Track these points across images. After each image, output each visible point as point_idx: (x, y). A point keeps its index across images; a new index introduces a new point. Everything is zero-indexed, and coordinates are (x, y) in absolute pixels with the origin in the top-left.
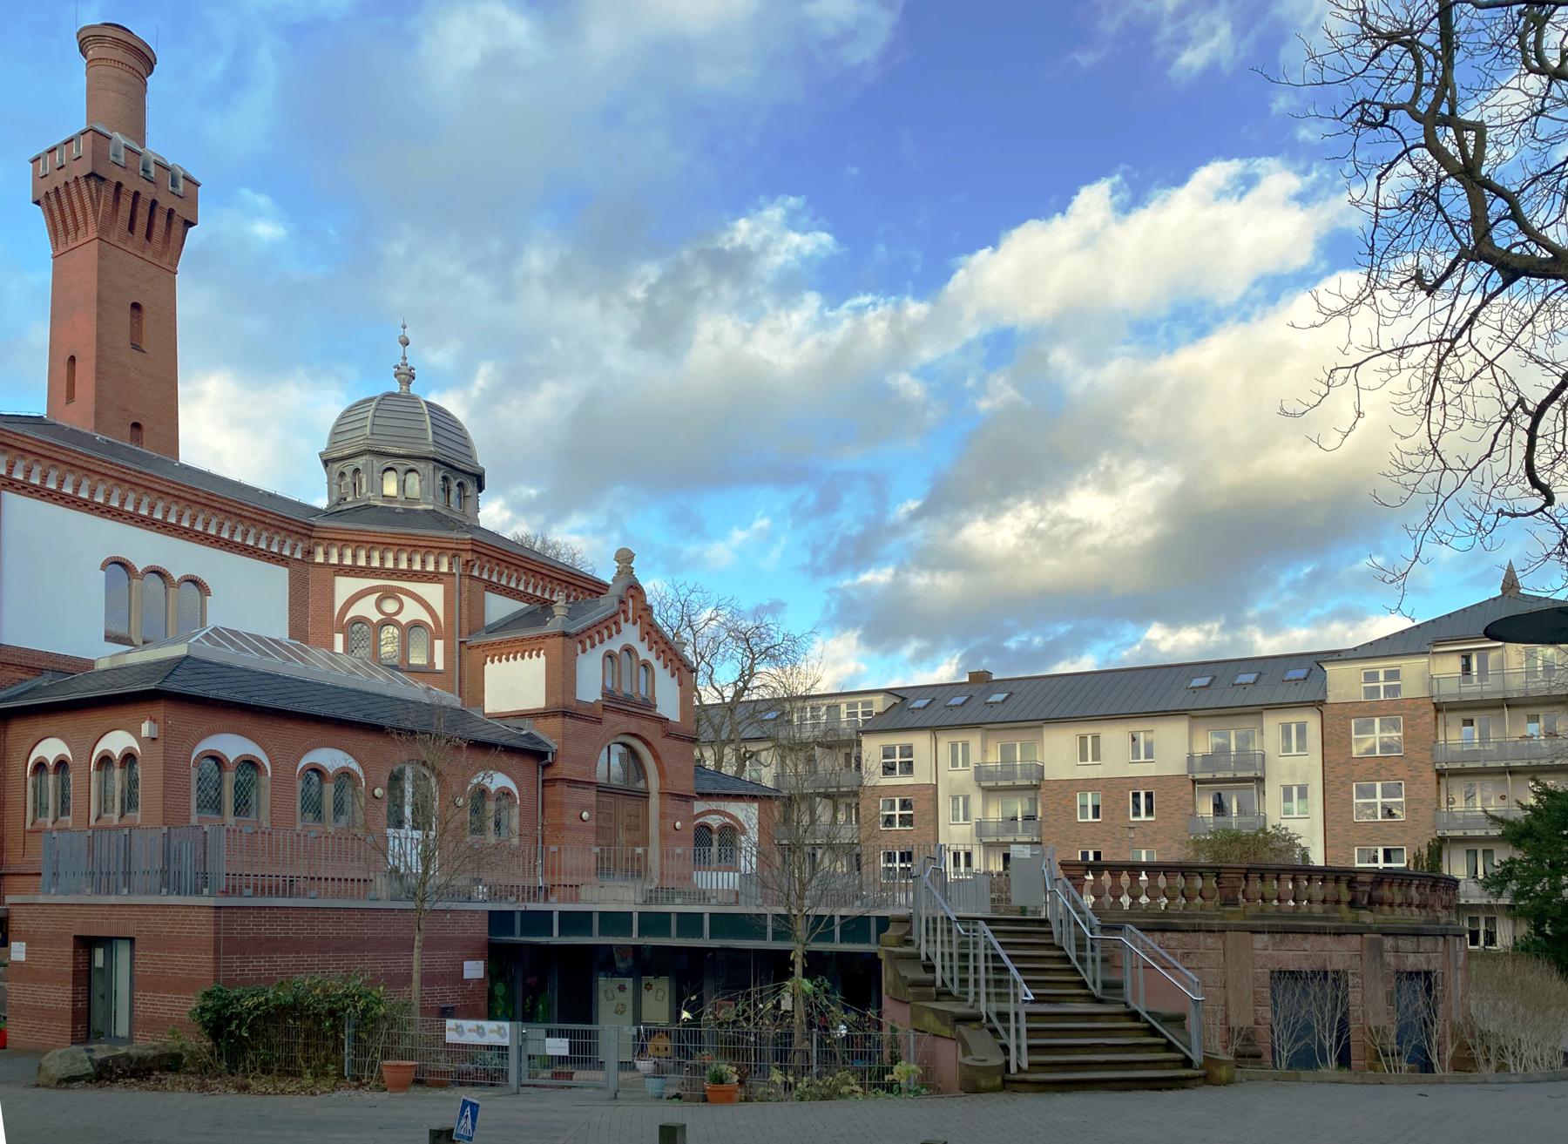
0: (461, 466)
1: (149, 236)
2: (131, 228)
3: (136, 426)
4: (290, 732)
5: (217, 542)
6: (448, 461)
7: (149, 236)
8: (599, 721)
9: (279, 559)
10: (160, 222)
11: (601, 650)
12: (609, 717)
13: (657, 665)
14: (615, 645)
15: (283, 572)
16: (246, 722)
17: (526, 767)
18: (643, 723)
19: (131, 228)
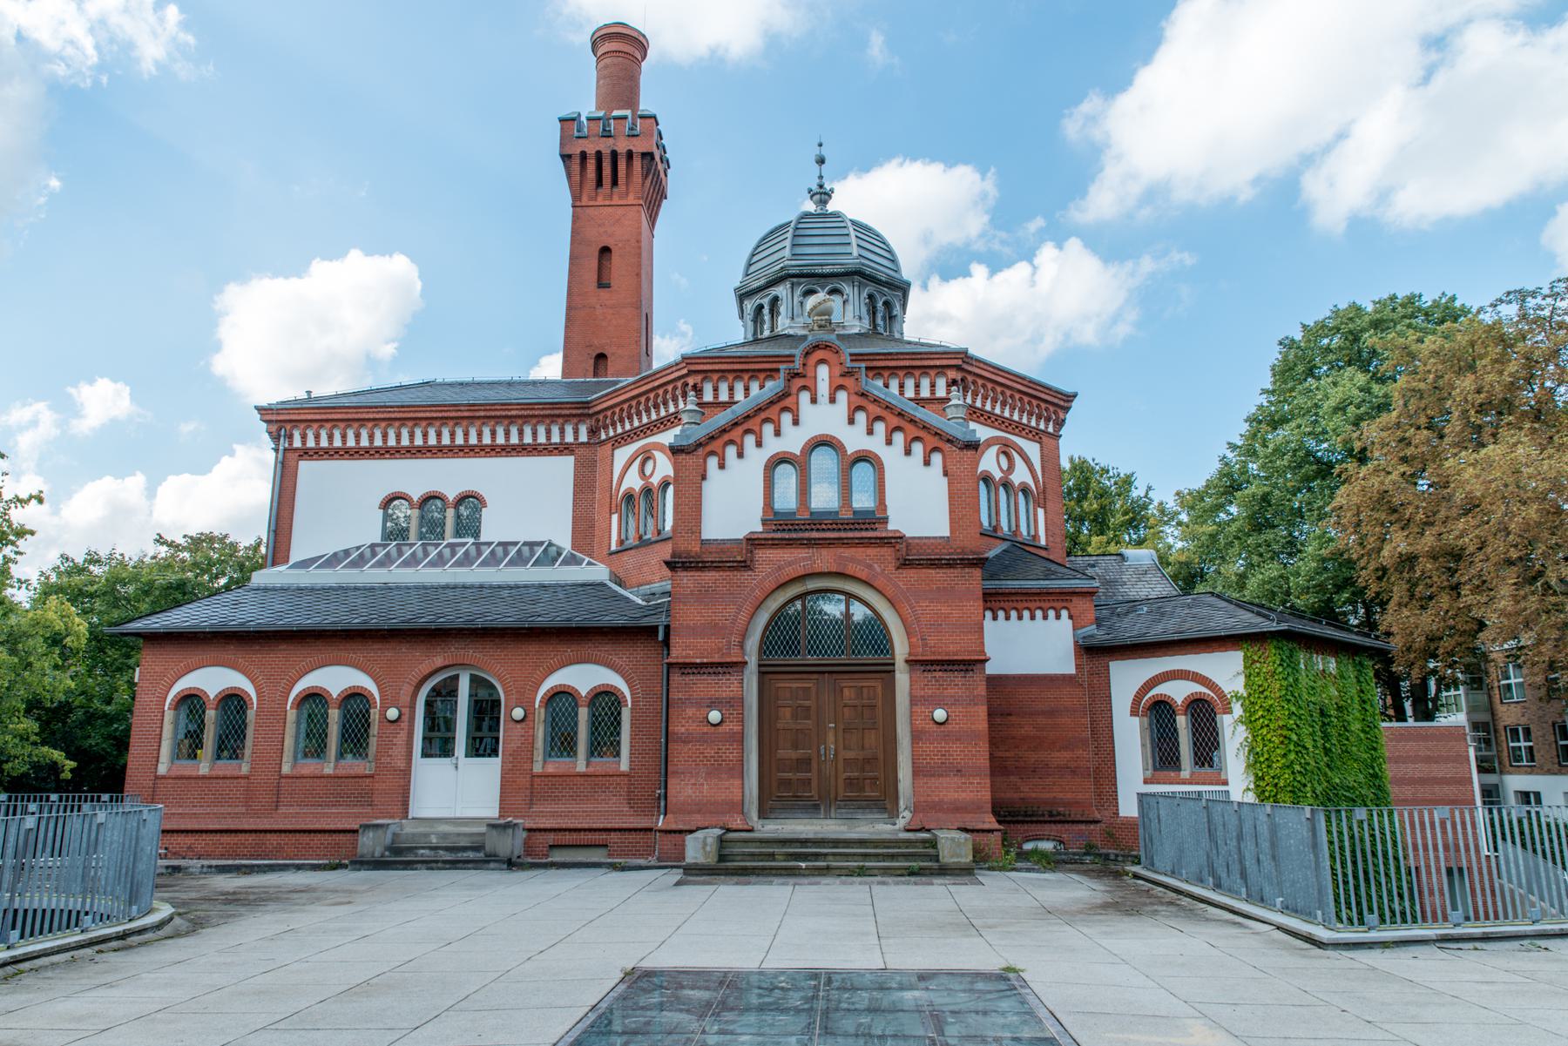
0: (827, 270)
1: (615, 183)
2: (599, 183)
3: (601, 357)
4: (278, 657)
5: (494, 451)
6: (806, 270)
7: (615, 183)
8: (745, 566)
9: (563, 449)
10: (622, 165)
11: (757, 458)
12: (762, 555)
13: (892, 456)
14: (793, 440)
15: (566, 464)
16: (231, 652)
17: (638, 654)
18: (847, 552)
19: (599, 183)
